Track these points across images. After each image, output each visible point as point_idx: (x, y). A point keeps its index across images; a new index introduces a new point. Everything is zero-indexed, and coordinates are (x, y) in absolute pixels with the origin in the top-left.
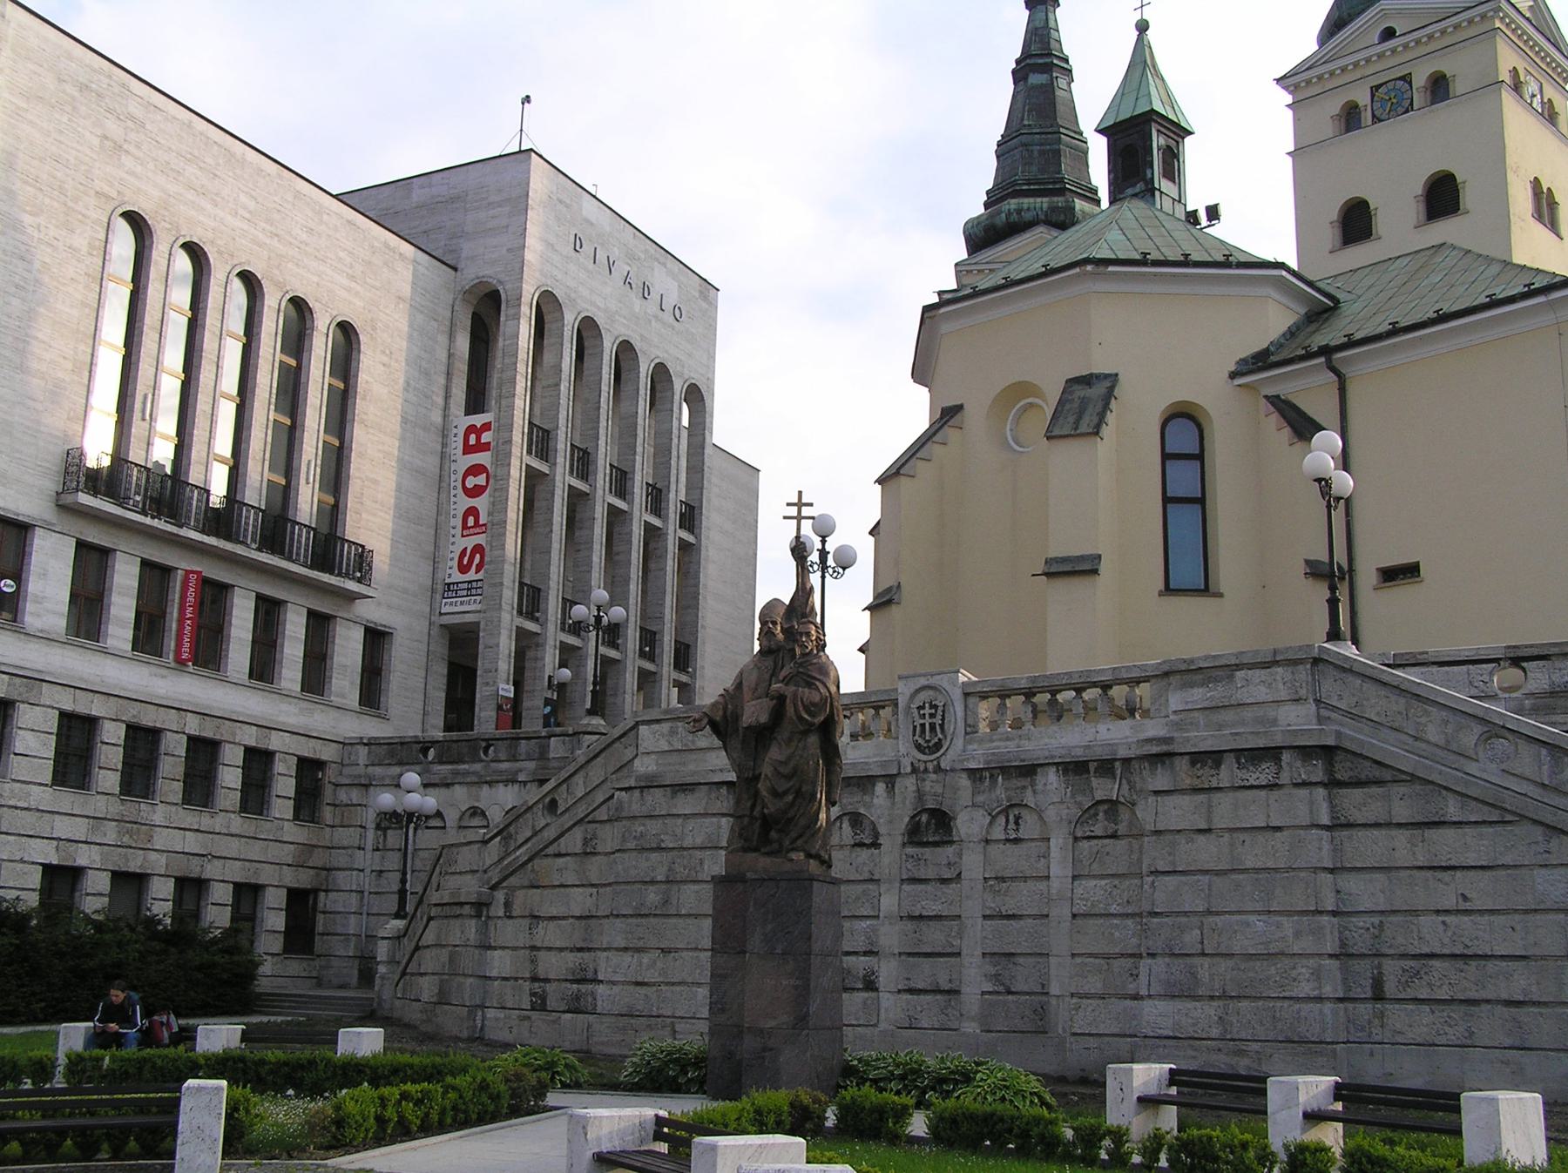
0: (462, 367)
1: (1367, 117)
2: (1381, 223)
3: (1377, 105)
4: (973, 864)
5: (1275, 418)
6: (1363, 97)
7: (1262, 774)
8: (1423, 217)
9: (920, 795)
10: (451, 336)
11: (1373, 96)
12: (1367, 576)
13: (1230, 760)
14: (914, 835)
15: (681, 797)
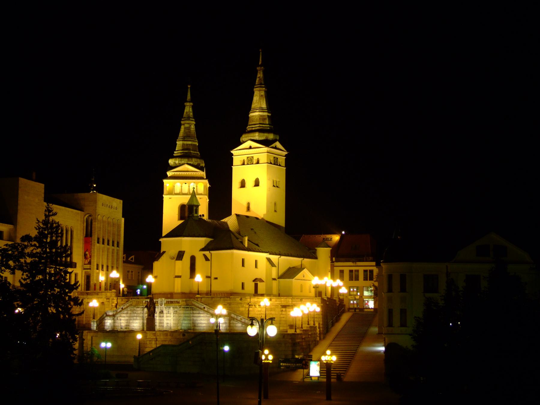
0: (85, 228)
1: (246, 163)
2: (247, 185)
3: (248, 161)
4: (165, 315)
5: (203, 257)
6: (246, 159)
7: (187, 309)
8: (254, 186)
9: (161, 309)
10: (84, 223)
11: (247, 159)
12: (212, 278)
13: (185, 308)
14: (160, 313)
15: (138, 308)
